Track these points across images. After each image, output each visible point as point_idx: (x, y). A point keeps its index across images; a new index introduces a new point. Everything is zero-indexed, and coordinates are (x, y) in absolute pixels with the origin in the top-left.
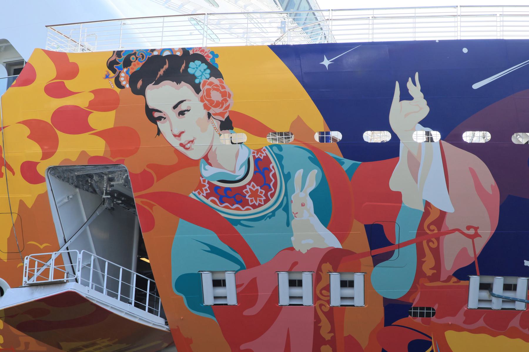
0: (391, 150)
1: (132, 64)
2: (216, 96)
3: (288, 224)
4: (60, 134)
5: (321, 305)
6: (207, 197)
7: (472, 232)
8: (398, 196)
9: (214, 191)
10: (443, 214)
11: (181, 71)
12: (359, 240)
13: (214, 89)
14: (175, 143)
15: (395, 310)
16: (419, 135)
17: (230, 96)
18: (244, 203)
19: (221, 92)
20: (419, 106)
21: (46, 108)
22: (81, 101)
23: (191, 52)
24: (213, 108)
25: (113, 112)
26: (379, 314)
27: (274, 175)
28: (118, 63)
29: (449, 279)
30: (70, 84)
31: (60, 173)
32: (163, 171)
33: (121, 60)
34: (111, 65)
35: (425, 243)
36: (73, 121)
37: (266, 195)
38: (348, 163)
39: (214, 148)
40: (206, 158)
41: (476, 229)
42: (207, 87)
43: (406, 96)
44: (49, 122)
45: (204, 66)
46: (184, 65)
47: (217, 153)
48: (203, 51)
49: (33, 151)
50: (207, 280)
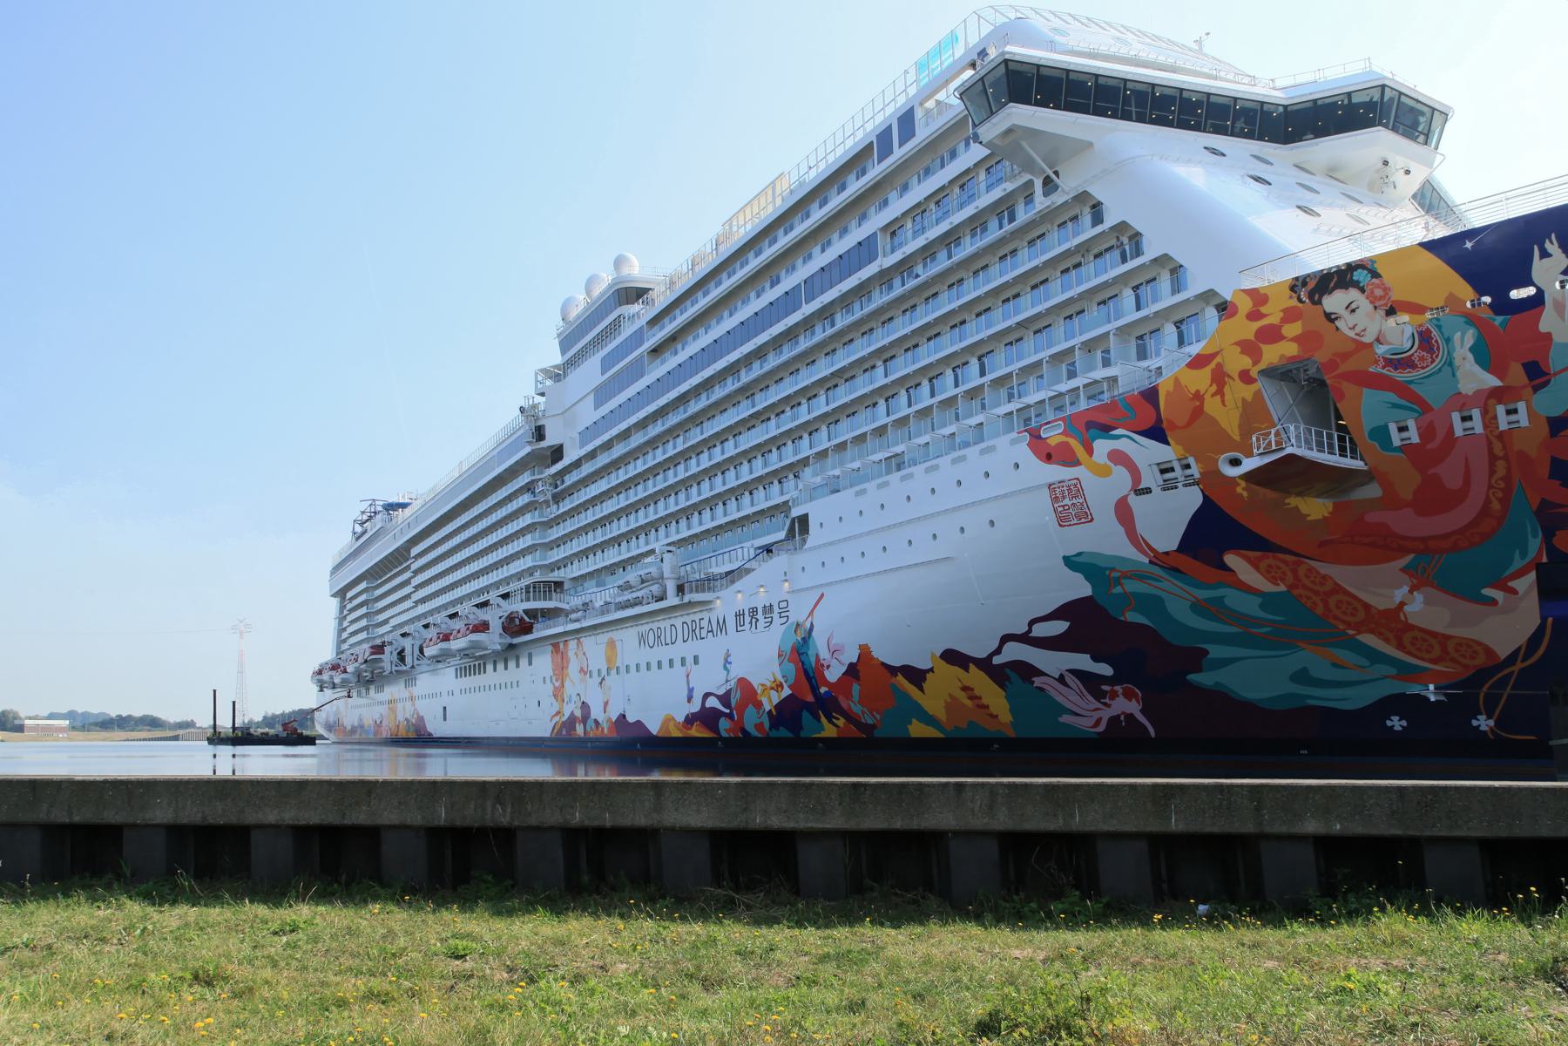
0: (1538, 301)
2: (1378, 292)
8: (1548, 337)
9: (1389, 363)
12: (1517, 374)
14: (1352, 334)
18: (1414, 367)
21: (1249, 330)
22: (1274, 319)
25: (1299, 323)
26: (1545, 429)
30: (1263, 310)
31: (1268, 373)
32: (1345, 356)
36: (1271, 335)
38: (1499, 320)
40: (1378, 340)
43: (1545, 254)
49: (1246, 362)
50: (1393, 428)
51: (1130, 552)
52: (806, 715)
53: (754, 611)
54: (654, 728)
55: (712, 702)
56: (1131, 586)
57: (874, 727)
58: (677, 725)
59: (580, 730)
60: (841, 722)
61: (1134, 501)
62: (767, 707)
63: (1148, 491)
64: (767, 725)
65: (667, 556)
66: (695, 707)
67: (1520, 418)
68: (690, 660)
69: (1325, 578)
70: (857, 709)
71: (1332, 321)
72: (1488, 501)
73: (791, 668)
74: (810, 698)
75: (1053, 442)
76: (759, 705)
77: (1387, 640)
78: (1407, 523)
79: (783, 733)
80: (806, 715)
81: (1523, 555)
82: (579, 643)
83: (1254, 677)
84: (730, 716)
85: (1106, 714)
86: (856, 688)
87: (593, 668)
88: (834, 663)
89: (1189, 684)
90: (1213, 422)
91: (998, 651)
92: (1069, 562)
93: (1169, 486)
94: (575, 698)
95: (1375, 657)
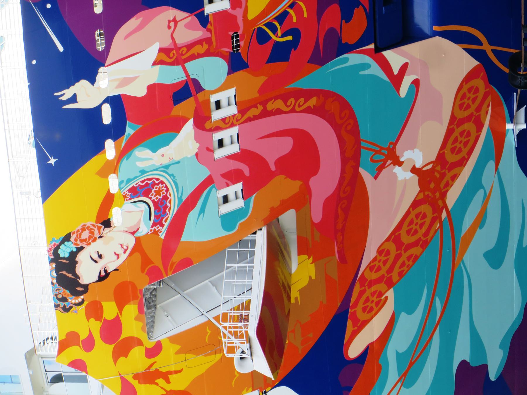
1: (64, 296)
3: (178, 162)
4: (123, 336)
5: (237, 120)
6: (162, 225)
7: (172, 24)
8: (151, 88)
9: (158, 222)
10: (161, 50)
11: (67, 262)
12: (187, 107)
13: (80, 237)
14: (124, 257)
15: (236, 64)
17: (85, 225)
19: (82, 232)
21: (103, 350)
22: (95, 326)
23: (53, 257)
24: (95, 235)
25: (104, 304)
26: (241, 74)
27: (142, 182)
28: (65, 306)
29: (209, 30)
30: (83, 336)
32: (146, 260)
33: (62, 304)
34: (66, 310)
35: (183, 57)
36: (112, 330)
37: (158, 184)
38: (130, 130)
39: (126, 229)
40: (133, 233)
41: (170, 22)
42: (78, 242)
43: (74, 99)
44: (113, 346)
45: (62, 246)
46: (63, 261)
47: (129, 226)
48: (50, 249)
67: (225, 101)
69: (380, 252)
71: (107, 274)
72: (308, 110)
77: (454, 178)
78: (325, 182)
81: (366, 66)
89: (501, 378)
90: (198, 381)
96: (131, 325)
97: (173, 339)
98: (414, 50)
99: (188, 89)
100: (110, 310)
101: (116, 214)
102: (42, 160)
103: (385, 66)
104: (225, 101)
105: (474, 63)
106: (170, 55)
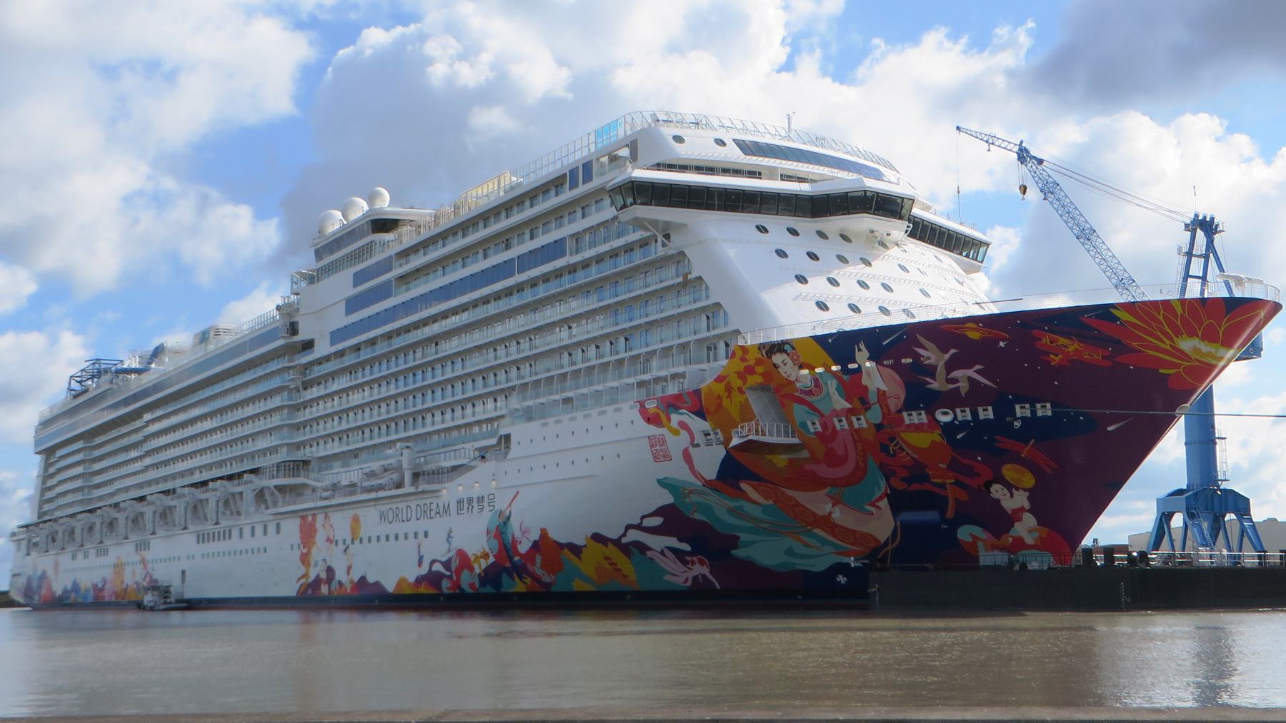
8: (866, 388)
12: (856, 401)
15: (879, 427)
16: (868, 364)
20: (866, 353)
21: (741, 367)
22: (752, 363)
26: (874, 431)
36: (750, 370)
38: (845, 377)
49: (739, 383)
51: (692, 479)
52: (505, 577)
53: (470, 500)
54: (390, 586)
55: (438, 567)
56: (694, 498)
57: (550, 584)
58: (409, 584)
59: (324, 589)
60: (528, 581)
61: (691, 450)
62: (478, 570)
63: (698, 445)
64: (477, 584)
65: (405, 452)
66: (424, 570)
67: (861, 423)
68: (421, 535)
70: (539, 572)
73: (495, 543)
74: (508, 565)
75: (651, 411)
76: (471, 569)
78: (823, 470)
79: (489, 589)
80: (505, 577)
82: (326, 516)
83: (766, 552)
84: (450, 577)
85: (691, 575)
86: (538, 558)
87: (339, 537)
88: (524, 540)
91: (624, 535)
92: (662, 483)
93: (709, 444)
94: (321, 563)
95: (824, 542)
96: (754, 380)
97: (747, 400)
98: (888, 512)
99: (866, 405)
100: (760, 369)
101: (805, 372)
102: (831, 335)
103: (880, 499)
104: (861, 423)
105: (882, 540)
106: (882, 395)
